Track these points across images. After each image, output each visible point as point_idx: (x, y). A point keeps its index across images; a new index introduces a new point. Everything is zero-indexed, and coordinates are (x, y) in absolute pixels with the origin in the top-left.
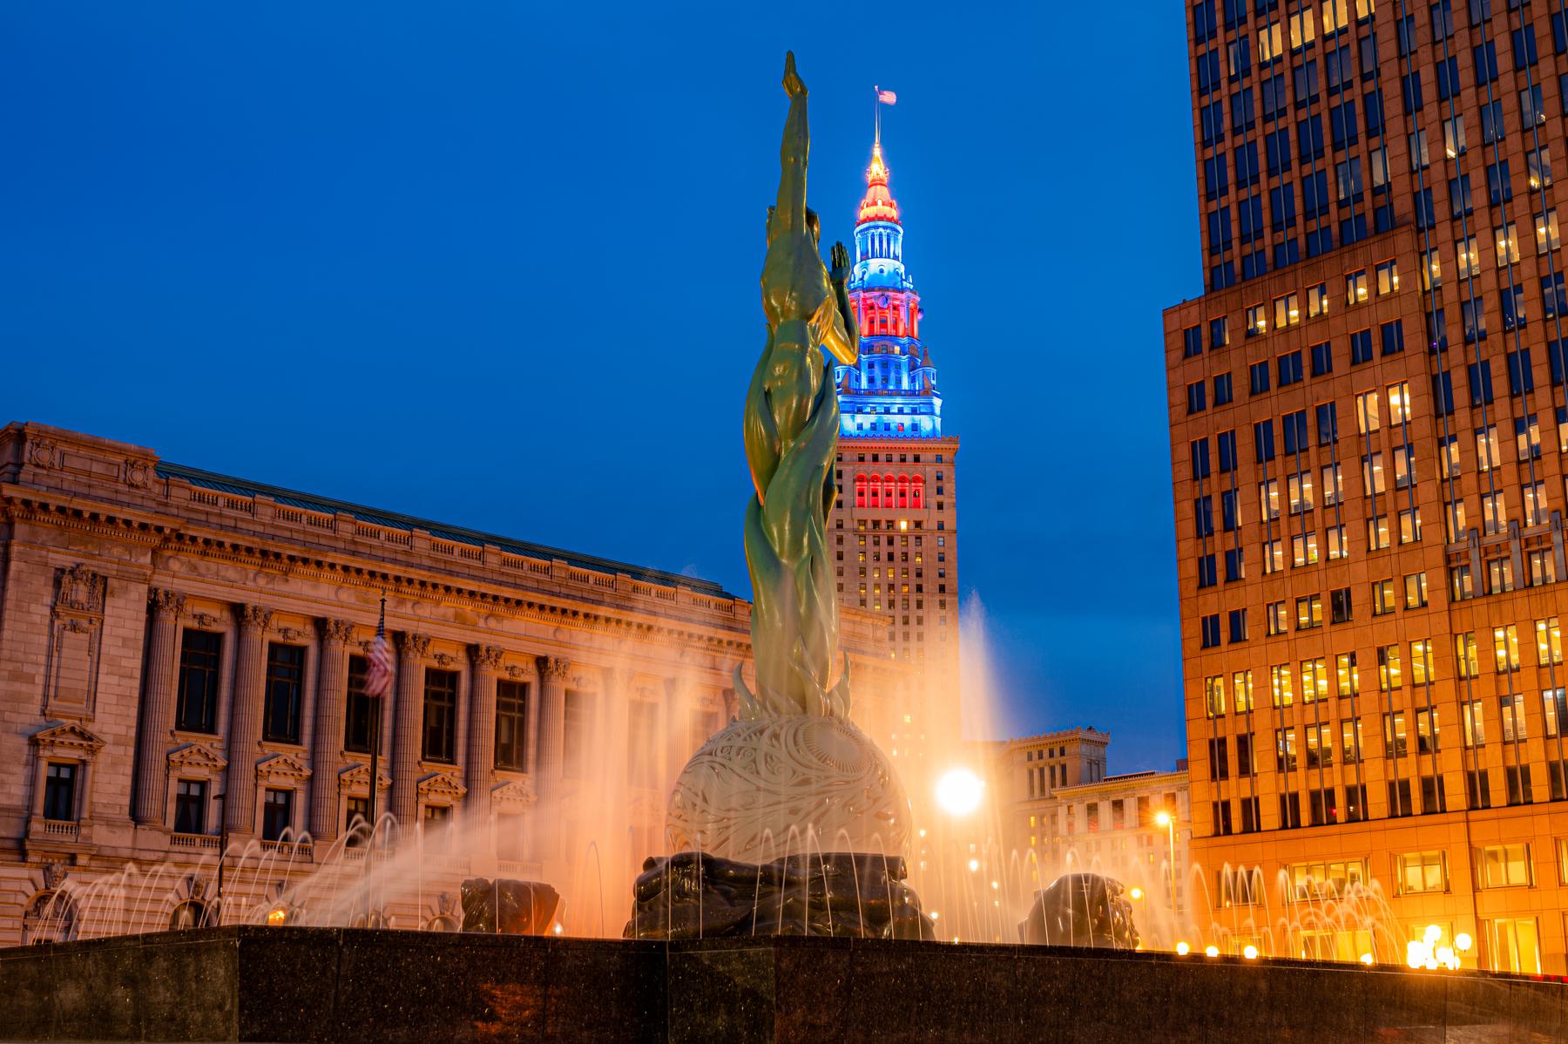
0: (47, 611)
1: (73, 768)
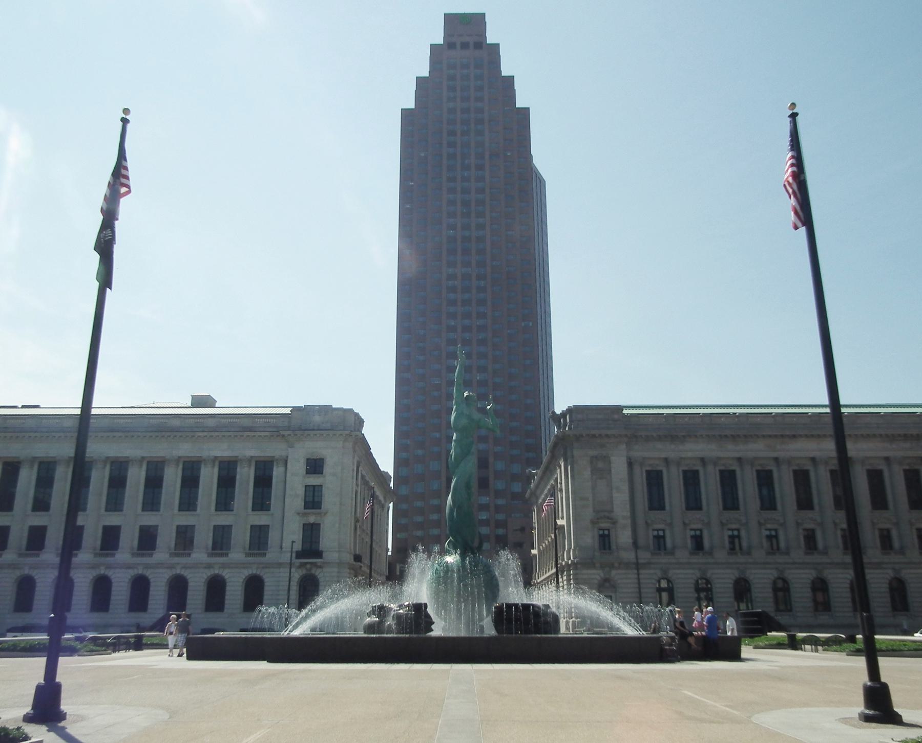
0: (589, 473)
1: (609, 530)
